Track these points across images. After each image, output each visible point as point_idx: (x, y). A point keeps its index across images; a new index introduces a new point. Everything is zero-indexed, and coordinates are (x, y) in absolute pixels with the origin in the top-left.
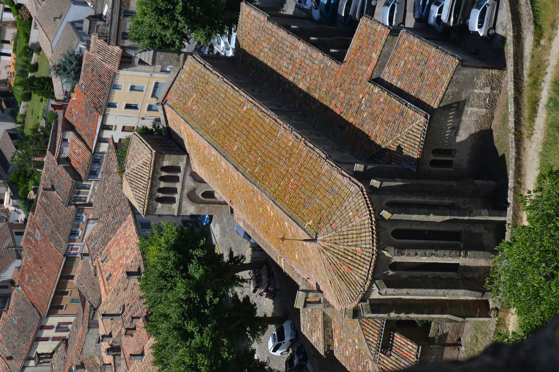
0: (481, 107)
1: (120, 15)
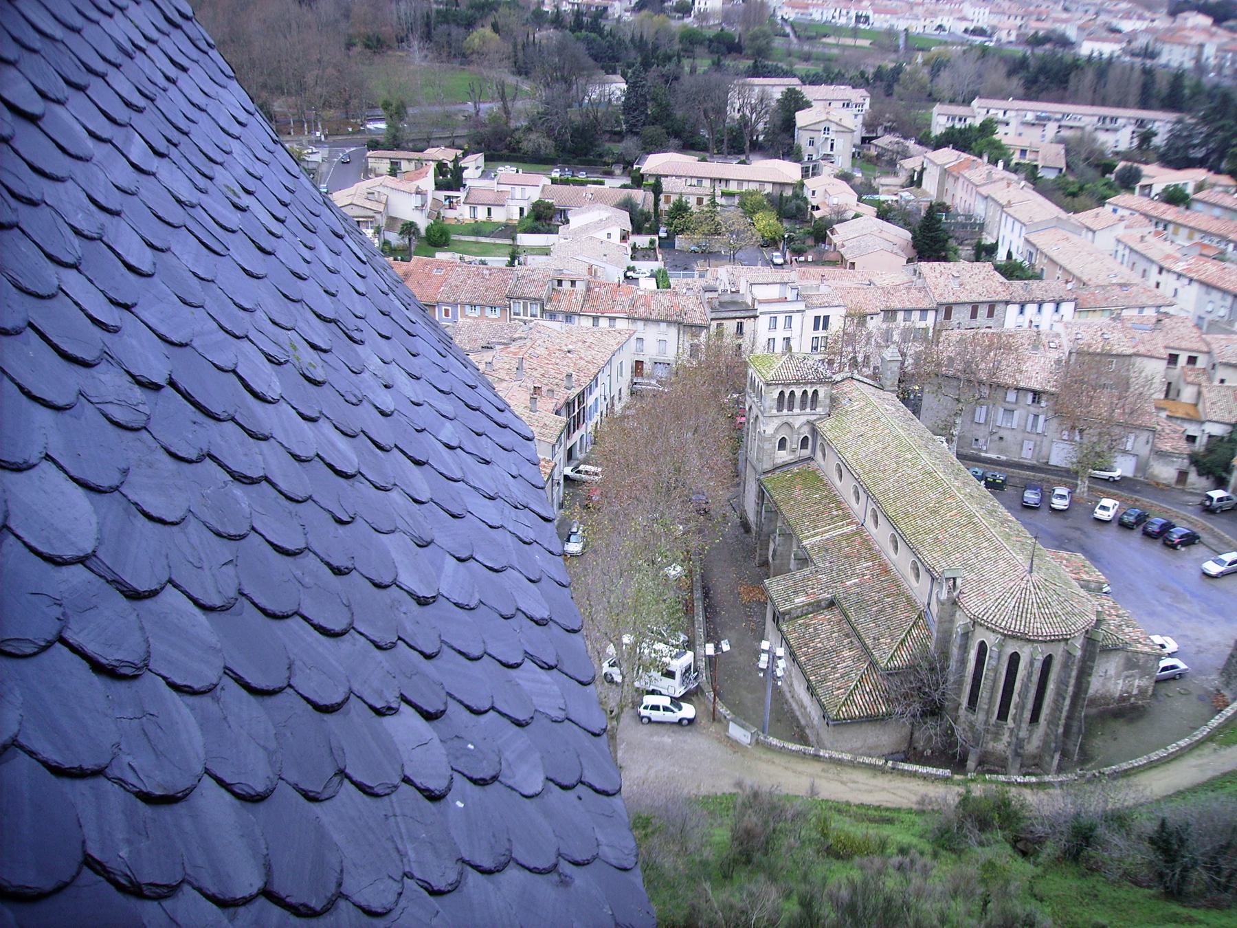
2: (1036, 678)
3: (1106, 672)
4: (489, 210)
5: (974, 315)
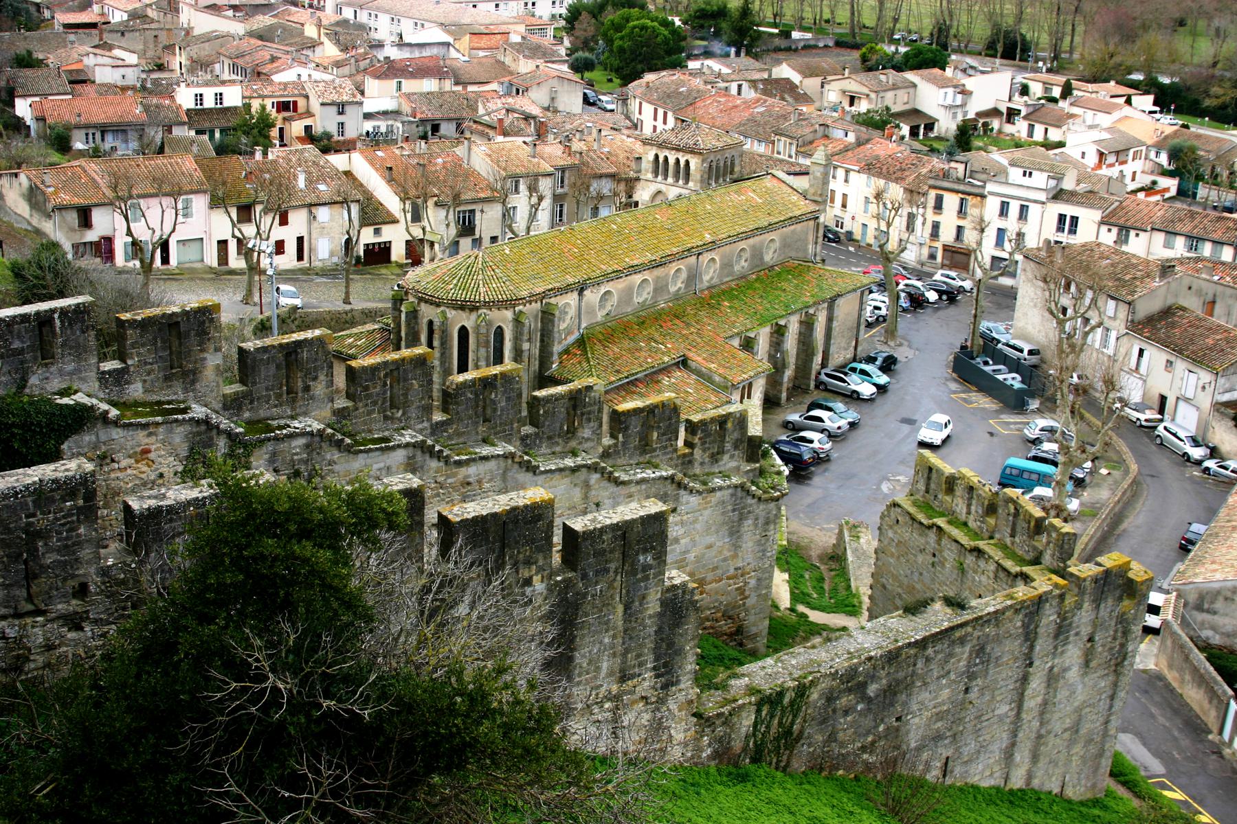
4: (1046, 130)
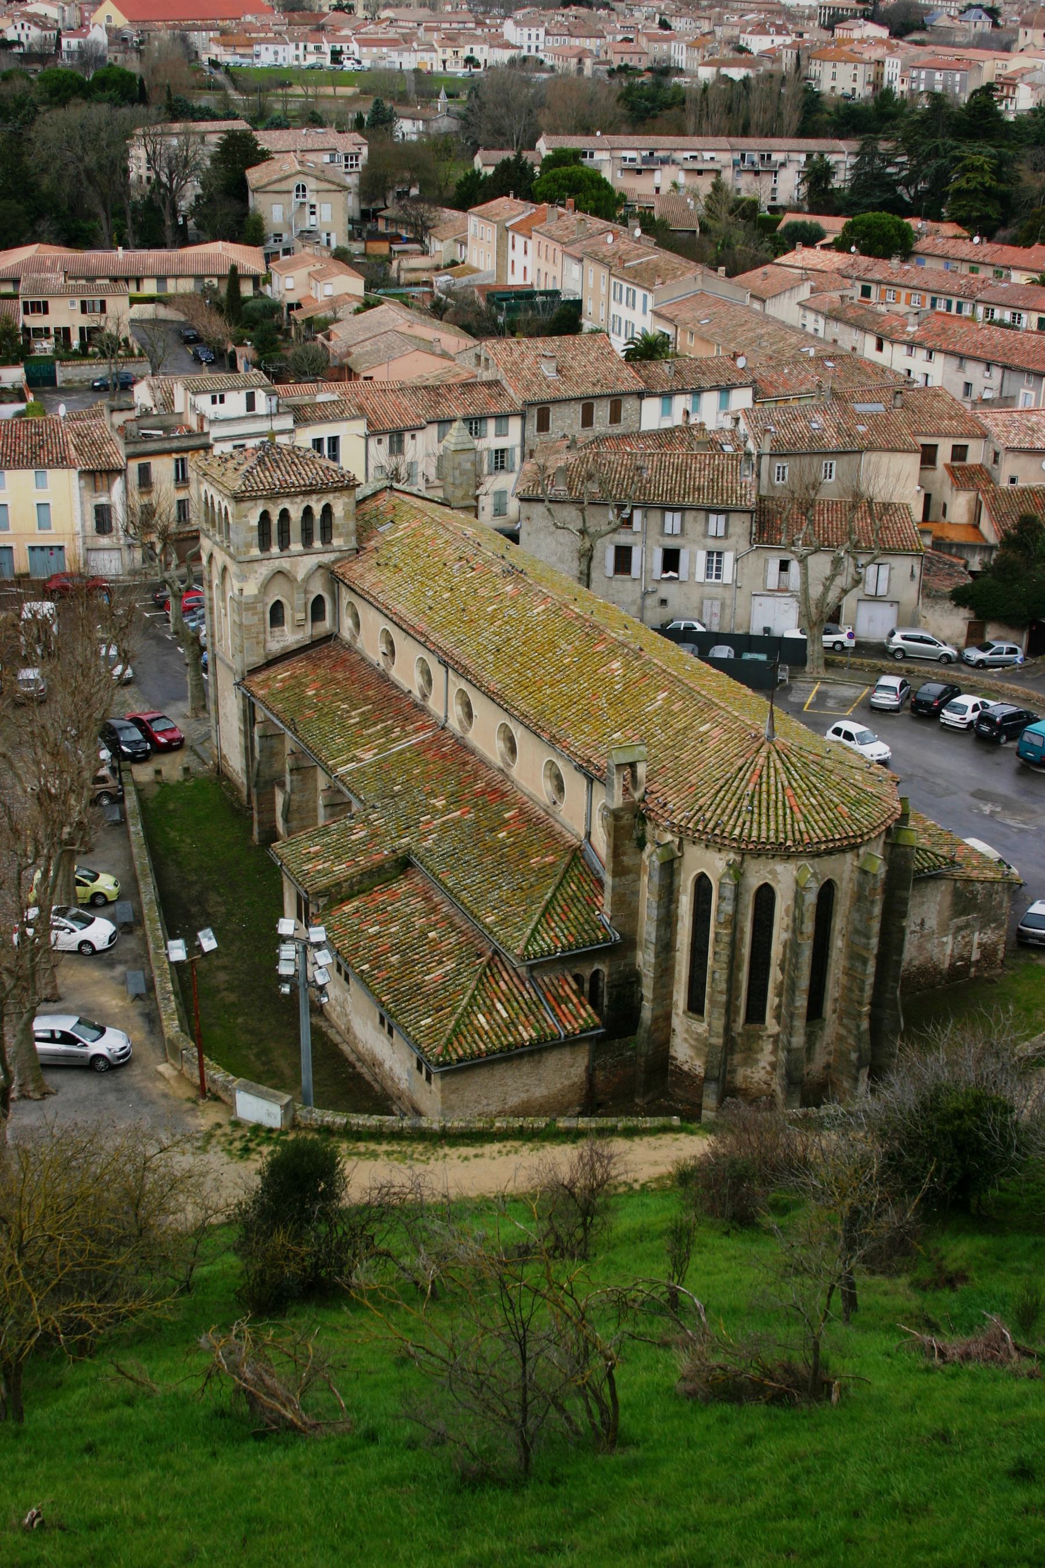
0: (952, 956)
1: (177, 451)
2: (809, 927)
3: (922, 924)
5: (587, 421)
